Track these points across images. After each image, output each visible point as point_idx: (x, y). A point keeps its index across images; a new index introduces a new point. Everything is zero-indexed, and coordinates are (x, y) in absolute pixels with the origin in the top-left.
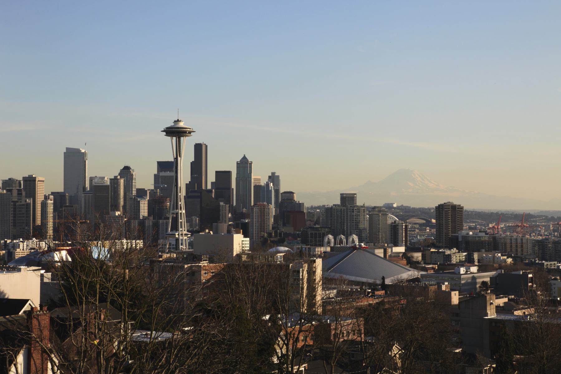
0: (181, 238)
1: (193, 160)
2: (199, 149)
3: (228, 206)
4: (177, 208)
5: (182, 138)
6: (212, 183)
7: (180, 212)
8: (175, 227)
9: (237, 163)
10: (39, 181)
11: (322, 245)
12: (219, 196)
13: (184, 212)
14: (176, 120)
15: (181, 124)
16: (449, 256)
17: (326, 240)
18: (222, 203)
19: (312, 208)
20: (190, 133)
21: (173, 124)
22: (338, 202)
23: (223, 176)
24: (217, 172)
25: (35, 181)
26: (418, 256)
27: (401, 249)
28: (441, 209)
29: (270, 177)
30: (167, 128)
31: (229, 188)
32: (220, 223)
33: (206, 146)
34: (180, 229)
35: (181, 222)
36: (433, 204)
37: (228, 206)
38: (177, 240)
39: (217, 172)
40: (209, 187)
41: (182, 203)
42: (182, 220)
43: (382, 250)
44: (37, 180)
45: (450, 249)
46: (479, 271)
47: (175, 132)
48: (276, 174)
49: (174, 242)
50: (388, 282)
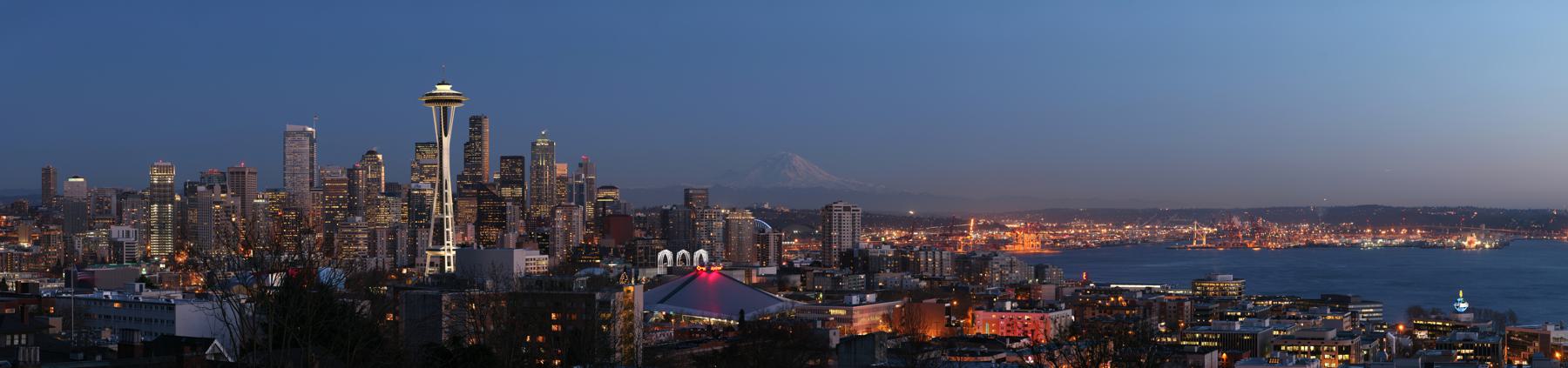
2: (476, 122)
8: (439, 240)
11: (655, 266)
13: (450, 216)
16: (839, 279)
17: (661, 255)
19: (643, 211)
22: (681, 202)
24: (503, 158)
26: (796, 279)
27: (773, 270)
28: (828, 208)
31: (522, 184)
36: (820, 206)
41: (450, 204)
42: (449, 230)
43: (743, 272)
45: (842, 268)
46: (878, 301)
49: (437, 261)
50: (748, 317)
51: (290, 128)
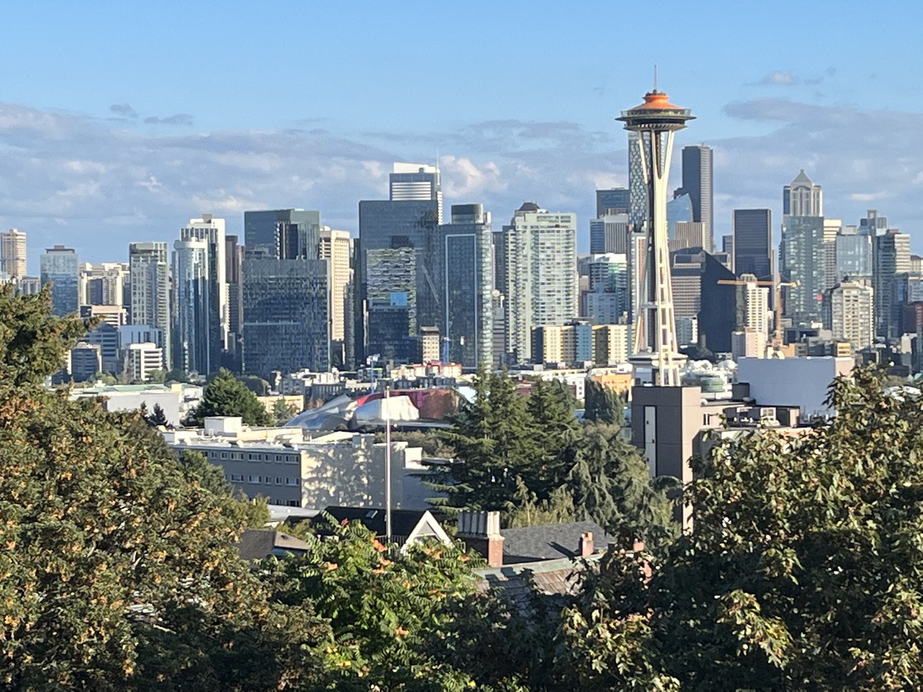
0: (663, 367)
1: (681, 186)
2: (692, 159)
3: (765, 291)
4: (653, 298)
5: (662, 134)
6: (724, 238)
7: (659, 305)
9: (786, 192)
10: (337, 239)
12: (745, 265)
14: (651, 92)
15: (661, 103)
18: (751, 286)
20: (681, 121)
21: (644, 102)
23: (751, 223)
25: (328, 240)
29: (864, 222)
30: (629, 112)
32: (749, 331)
33: (711, 151)
34: (661, 347)
35: (664, 331)
37: (765, 291)
38: (656, 371)
39: (737, 212)
40: (719, 250)
44: (333, 238)
47: (648, 120)
48: (879, 216)
51: (400, 168)
